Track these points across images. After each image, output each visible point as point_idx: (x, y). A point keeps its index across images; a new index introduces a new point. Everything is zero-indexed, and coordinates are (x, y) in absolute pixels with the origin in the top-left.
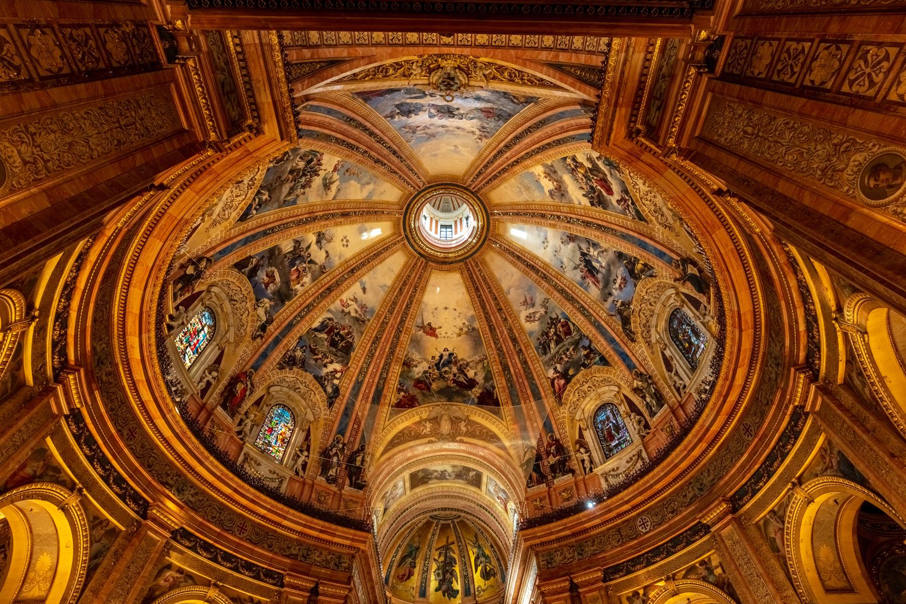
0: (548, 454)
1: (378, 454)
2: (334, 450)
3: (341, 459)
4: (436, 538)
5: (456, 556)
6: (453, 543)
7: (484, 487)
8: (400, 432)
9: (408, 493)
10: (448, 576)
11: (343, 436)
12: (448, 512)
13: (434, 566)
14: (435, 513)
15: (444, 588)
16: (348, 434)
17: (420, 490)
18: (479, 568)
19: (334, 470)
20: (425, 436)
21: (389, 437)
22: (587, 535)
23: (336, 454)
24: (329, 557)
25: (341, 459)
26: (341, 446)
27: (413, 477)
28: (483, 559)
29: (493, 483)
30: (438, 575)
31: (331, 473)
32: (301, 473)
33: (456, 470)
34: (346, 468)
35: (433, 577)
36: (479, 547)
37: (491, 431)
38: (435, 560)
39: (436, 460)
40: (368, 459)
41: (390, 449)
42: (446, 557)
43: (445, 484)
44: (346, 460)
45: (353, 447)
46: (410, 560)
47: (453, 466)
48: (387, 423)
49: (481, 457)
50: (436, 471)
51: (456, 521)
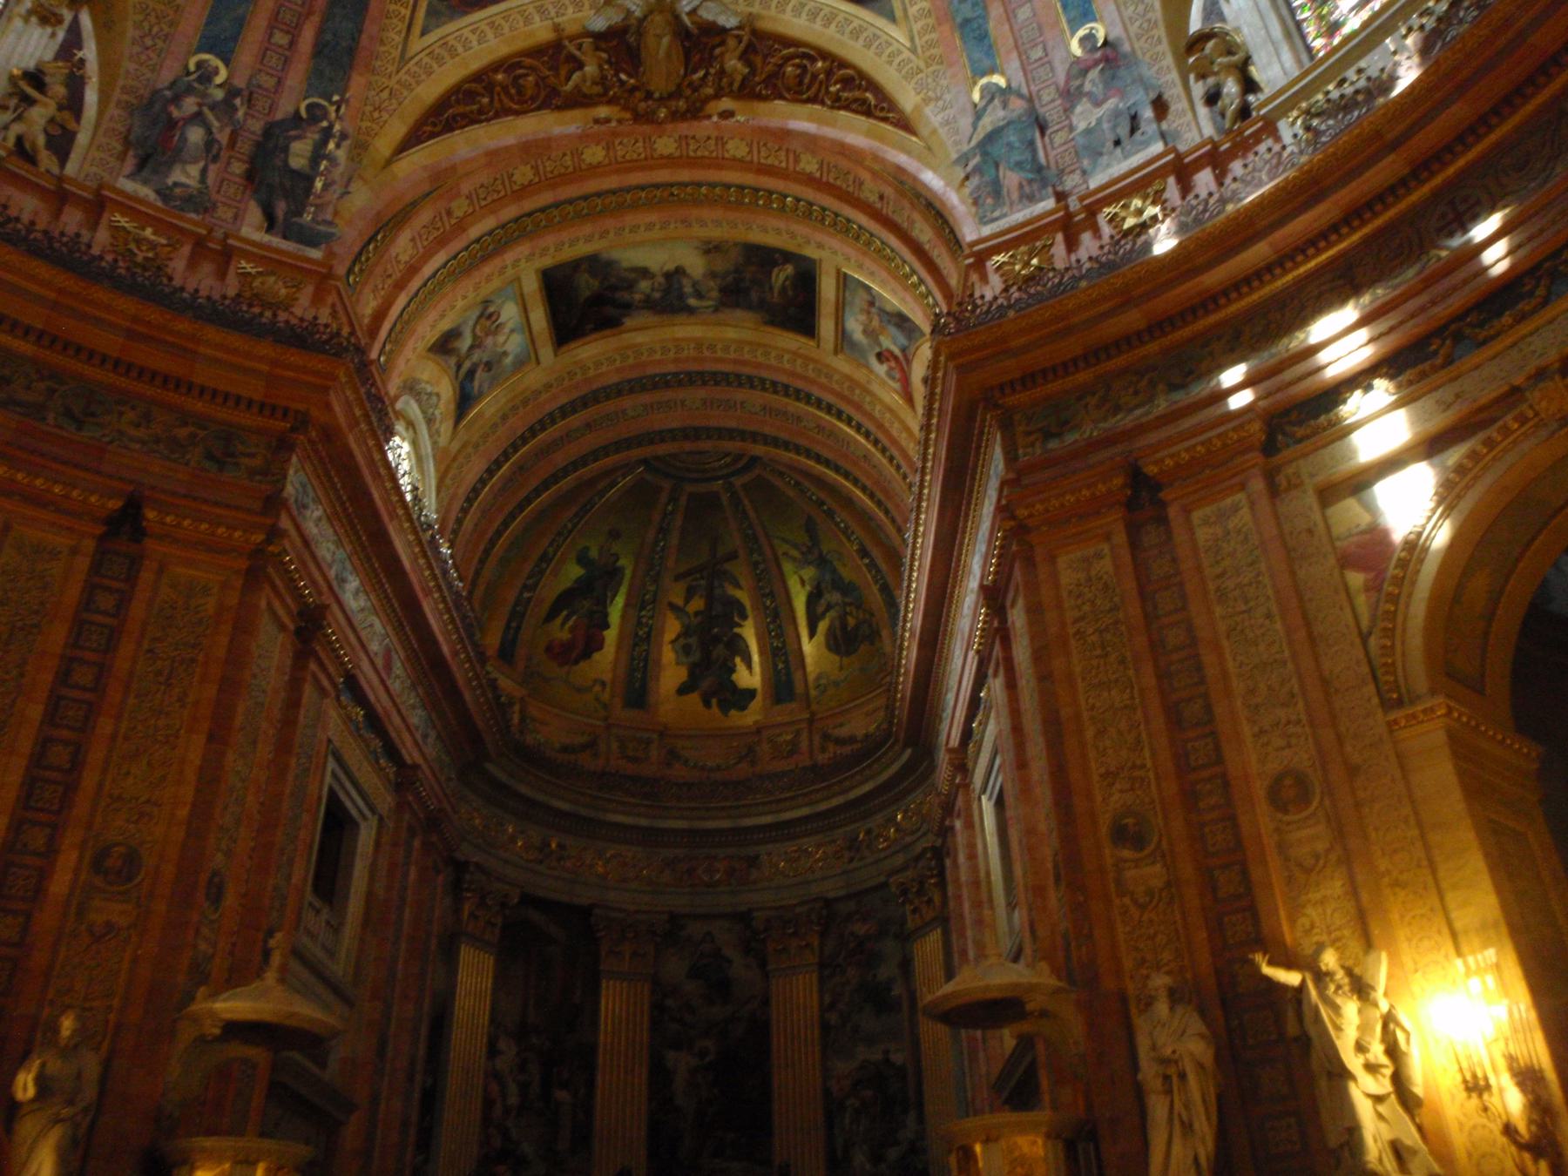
0: (1070, 96)
1: (384, 145)
2: (190, 105)
3: (223, 137)
4: (674, 540)
5: (743, 596)
6: (733, 556)
7: (826, 326)
8: (477, 77)
9: (546, 352)
10: (719, 651)
11: (227, 62)
12: (705, 445)
13: (672, 627)
14: (662, 449)
15: (706, 684)
16: (246, 56)
17: (591, 351)
18: (823, 626)
19: (194, 170)
20: (578, 100)
21: (430, 90)
22: (1212, 319)
23: (198, 117)
24: (182, 433)
25: (223, 137)
26: (219, 95)
27: (556, 285)
28: (835, 597)
29: (860, 299)
30: (687, 650)
31: (177, 176)
32: (47, 161)
33: (721, 265)
34: (250, 176)
35: (668, 655)
36: (822, 562)
37: (844, 64)
38: (672, 607)
39: (635, 206)
40: (341, 154)
41: (433, 135)
42: (710, 599)
43: (686, 330)
44: (245, 147)
45: (272, 108)
46: (587, 604)
47: (711, 249)
48: (417, 44)
49: (810, 180)
50: (644, 273)
51: (738, 482)
